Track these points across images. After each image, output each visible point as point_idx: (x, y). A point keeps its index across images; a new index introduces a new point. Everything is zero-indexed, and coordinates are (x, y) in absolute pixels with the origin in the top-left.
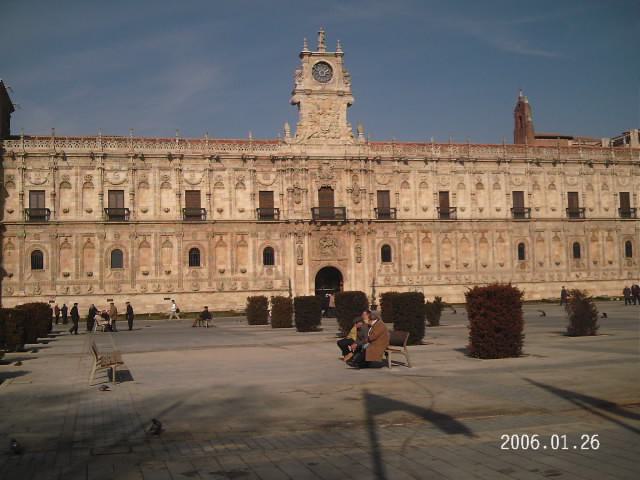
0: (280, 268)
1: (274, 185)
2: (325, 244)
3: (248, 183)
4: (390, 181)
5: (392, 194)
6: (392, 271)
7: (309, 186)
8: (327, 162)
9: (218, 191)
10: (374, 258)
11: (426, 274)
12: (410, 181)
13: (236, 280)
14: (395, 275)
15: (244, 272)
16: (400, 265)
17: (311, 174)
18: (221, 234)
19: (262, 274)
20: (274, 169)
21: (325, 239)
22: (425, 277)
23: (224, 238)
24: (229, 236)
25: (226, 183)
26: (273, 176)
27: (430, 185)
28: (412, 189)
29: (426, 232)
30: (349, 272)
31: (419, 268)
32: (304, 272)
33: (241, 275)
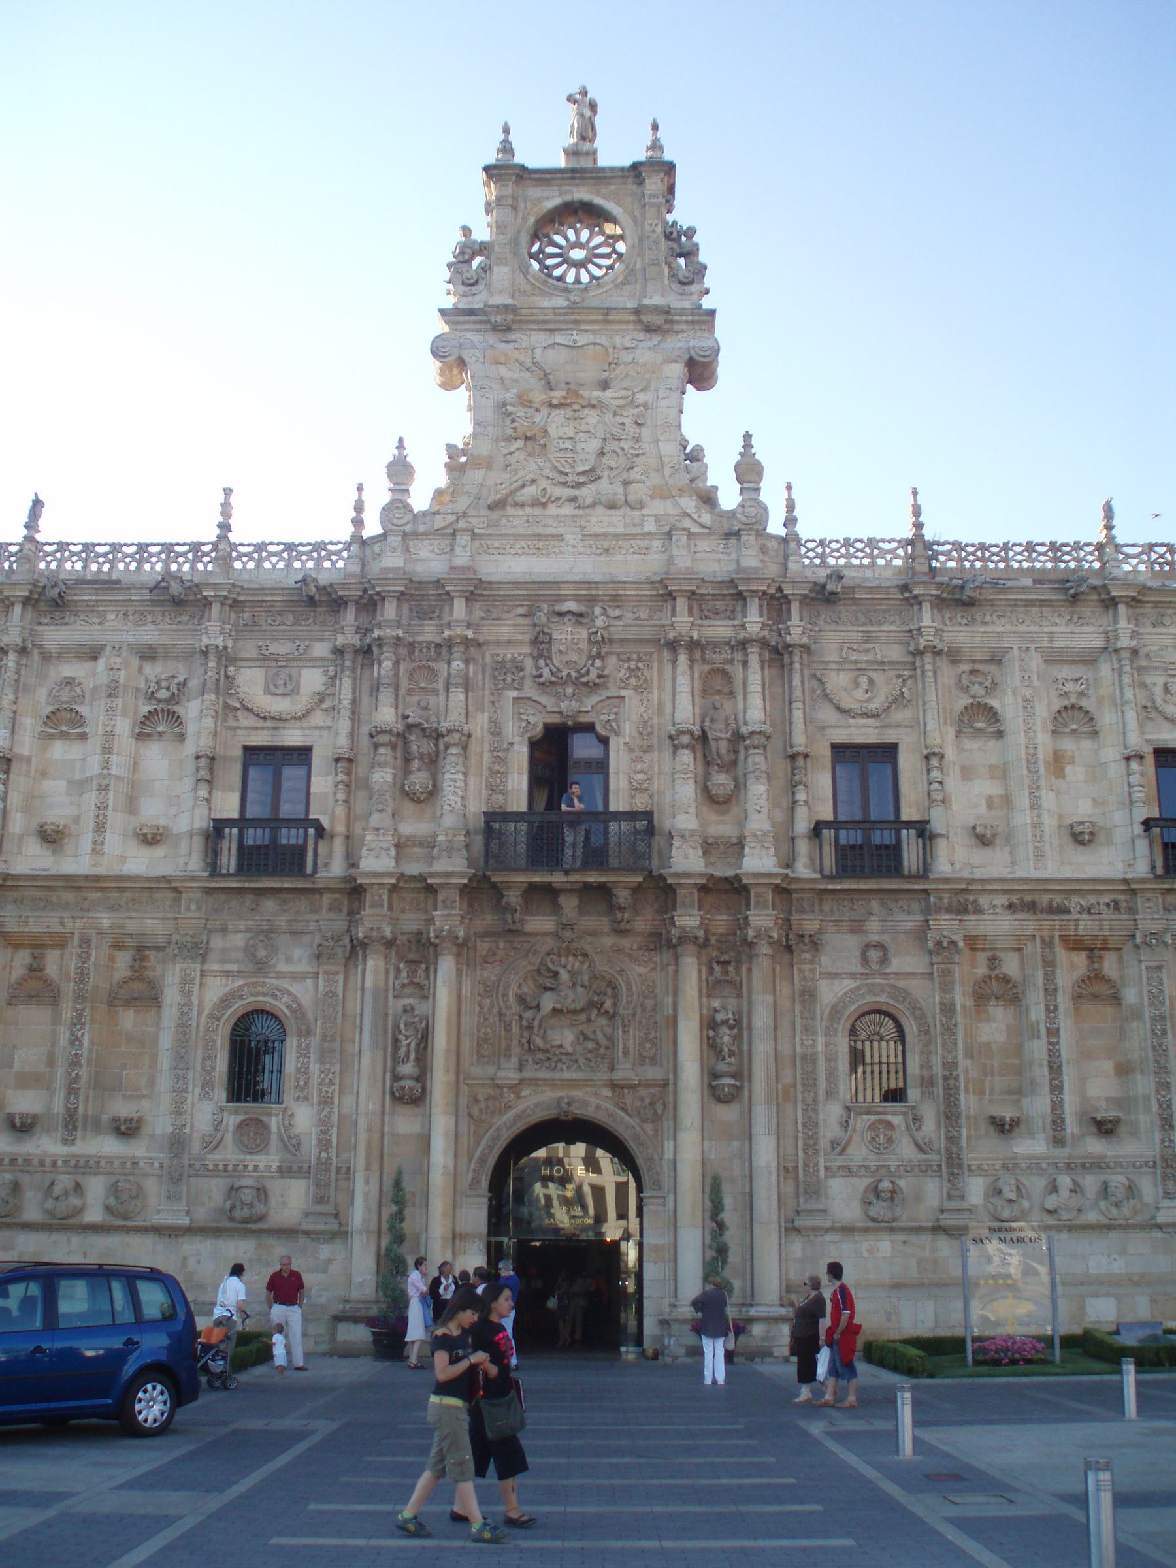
0: (304, 1118)
1: (318, 718)
2: (548, 1002)
3: (191, 710)
4: (899, 700)
5: (907, 762)
6: (906, 1150)
7: (479, 725)
8: (571, 606)
9: (59, 750)
10: (810, 1084)
11: (1099, 1165)
12: (1007, 704)
13: (84, 1167)
14: (925, 1169)
15: (127, 1130)
16: (951, 1115)
17: (500, 666)
18: (38, 946)
19: (212, 1144)
20: (321, 649)
21: (547, 979)
22: (1091, 1182)
23: (52, 964)
24: (73, 949)
25: (93, 713)
26: (312, 680)
27: (1107, 718)
28: (1017, 739)
29: (1093, 949)
30: (668, 1155)
31: (1058, 1141)
32: (424, 1141)
33: (110, 1146)
